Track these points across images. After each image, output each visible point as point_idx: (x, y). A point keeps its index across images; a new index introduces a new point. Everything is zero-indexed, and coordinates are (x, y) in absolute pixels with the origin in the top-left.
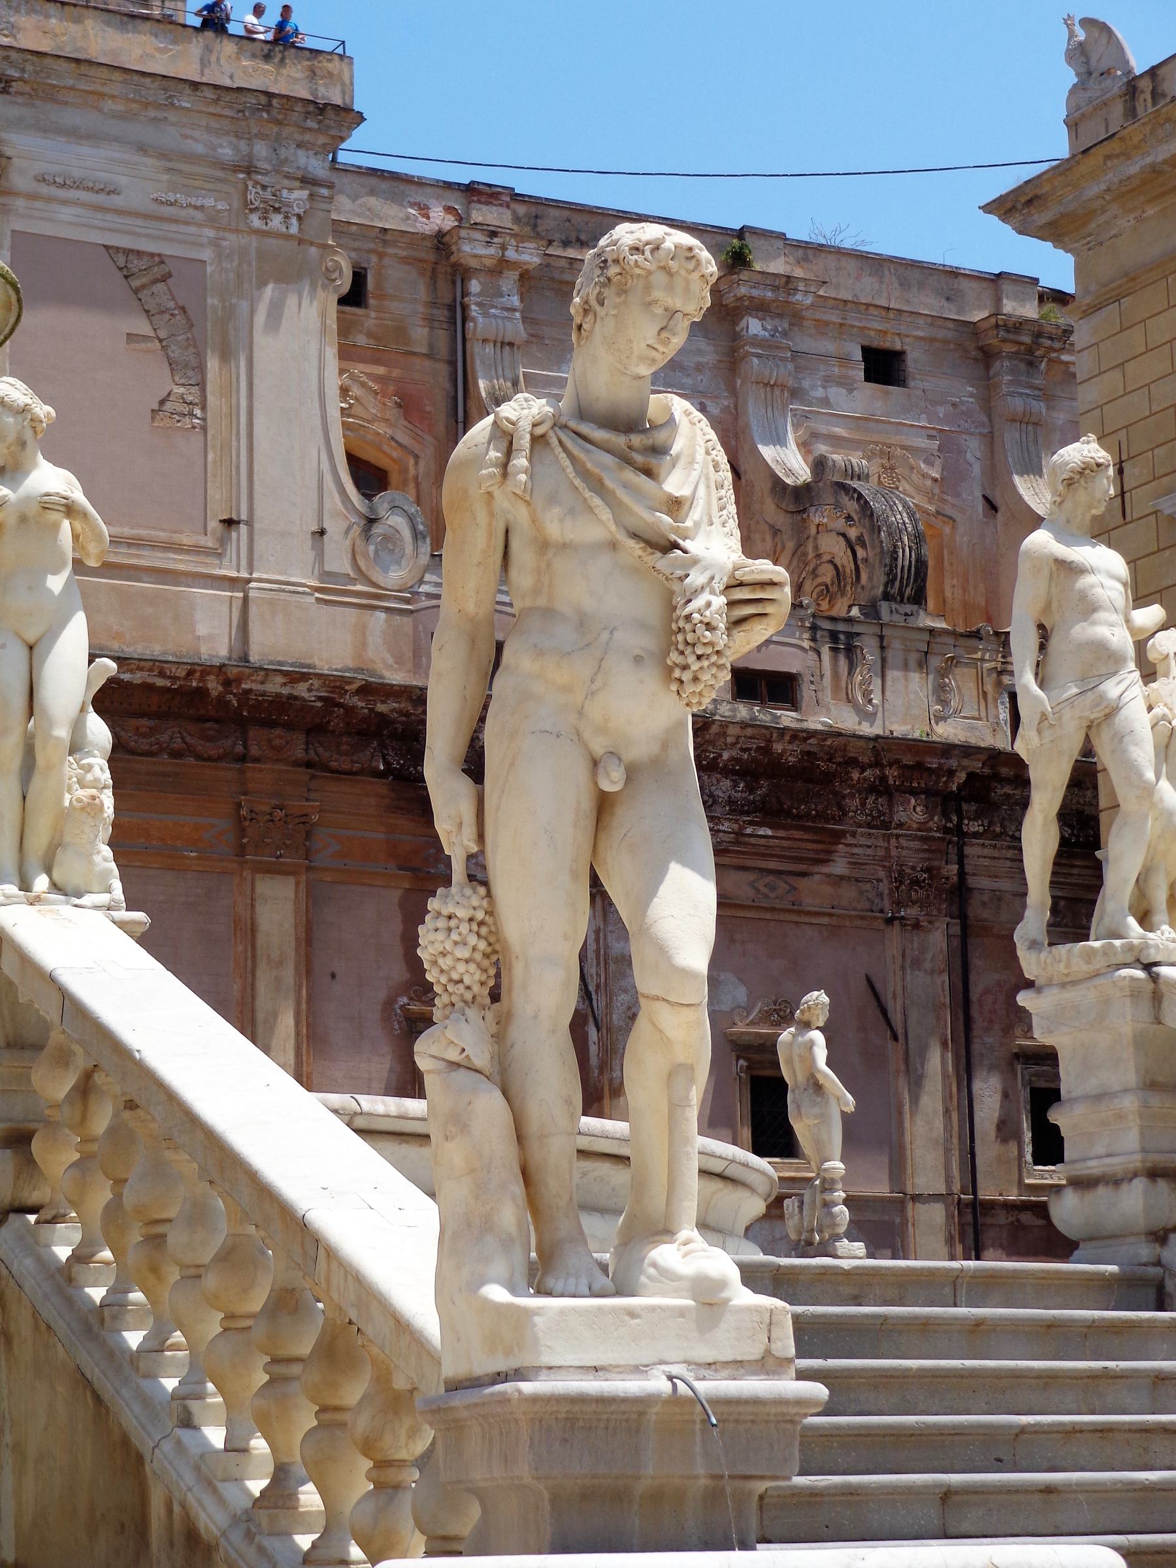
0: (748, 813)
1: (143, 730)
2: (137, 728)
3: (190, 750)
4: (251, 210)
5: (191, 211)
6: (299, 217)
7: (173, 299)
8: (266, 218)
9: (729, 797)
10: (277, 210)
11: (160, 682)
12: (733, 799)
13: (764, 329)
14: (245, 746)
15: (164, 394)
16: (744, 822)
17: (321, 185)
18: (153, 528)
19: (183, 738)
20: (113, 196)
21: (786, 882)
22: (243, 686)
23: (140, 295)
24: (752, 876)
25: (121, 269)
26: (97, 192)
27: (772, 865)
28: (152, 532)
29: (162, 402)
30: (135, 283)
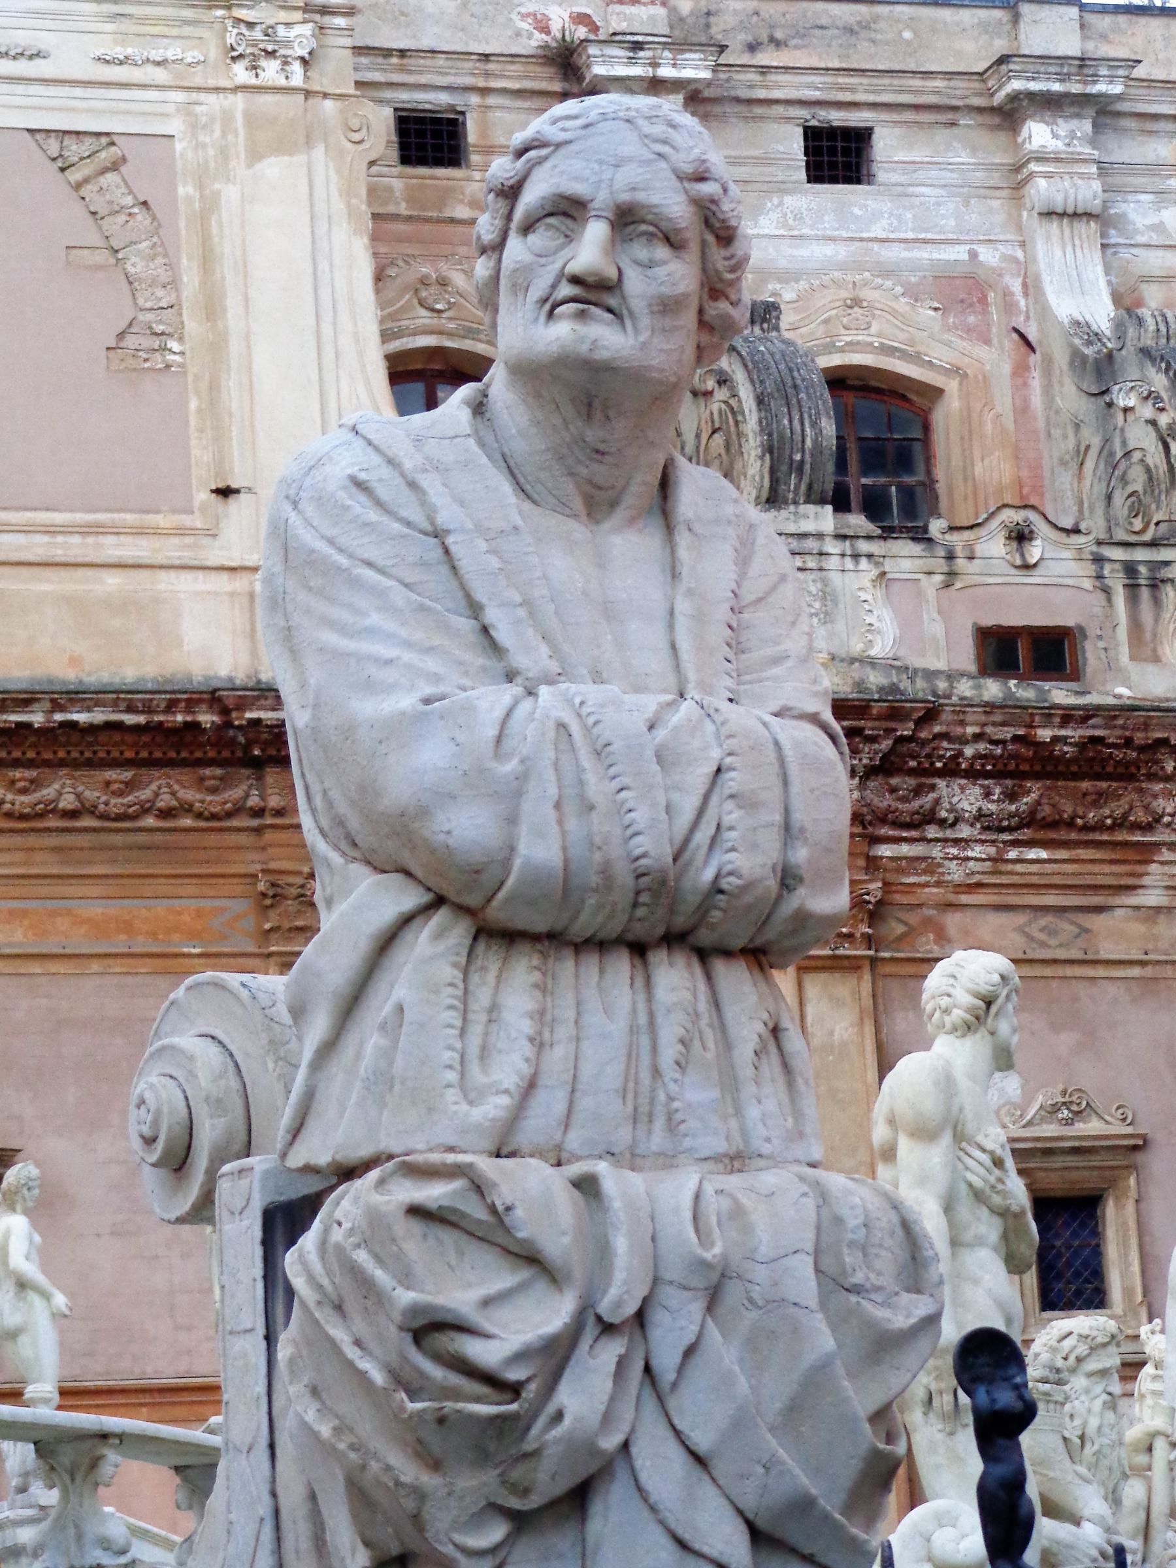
0: (1010, 829)
1: (115, 786)
2: (108, 784)
3: (187, 809)
4: (233, 59)
5: (150, 69)
6: (304, 61)
7: (131, 192)
8: (255, 68)
9: (980, 809)
10: (271, 54)
11: (130, 719)
12: (985, 811)
13: (1055, 136)
14: (263, 797)
15: (123, 325)
16: (1004, 842)
17: (333, 13)
18: (118, 511)
19: (173, 794)
20: (38, 62)
21: (1073, 923)
22: (249, 715)
23: (83, 192)
24: (1020, 919)
25: (54, 159)
26: (14, 58)
27: (1051, 899)
28: (116, 516)
29: (121, 335)
30: (75, 176)
